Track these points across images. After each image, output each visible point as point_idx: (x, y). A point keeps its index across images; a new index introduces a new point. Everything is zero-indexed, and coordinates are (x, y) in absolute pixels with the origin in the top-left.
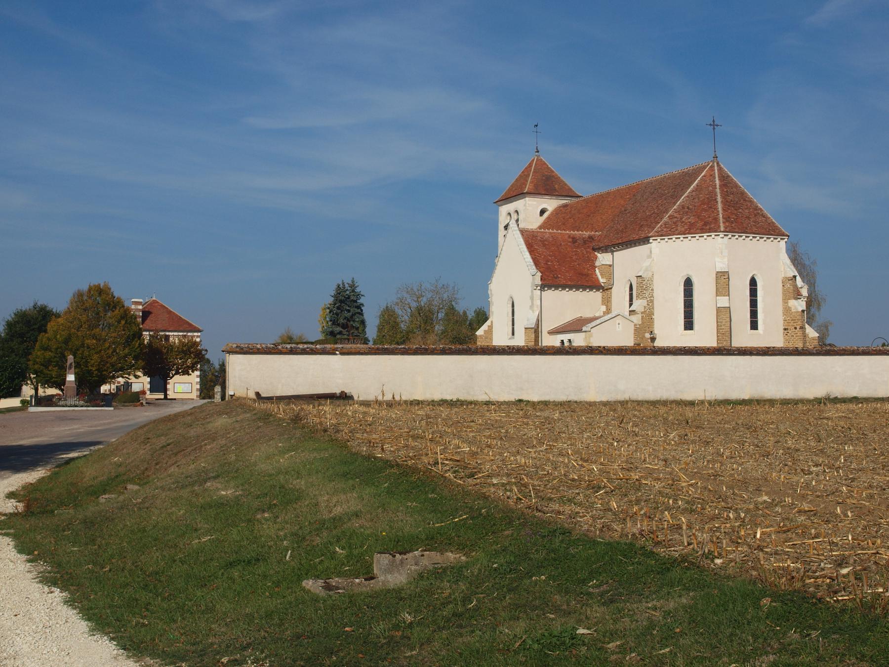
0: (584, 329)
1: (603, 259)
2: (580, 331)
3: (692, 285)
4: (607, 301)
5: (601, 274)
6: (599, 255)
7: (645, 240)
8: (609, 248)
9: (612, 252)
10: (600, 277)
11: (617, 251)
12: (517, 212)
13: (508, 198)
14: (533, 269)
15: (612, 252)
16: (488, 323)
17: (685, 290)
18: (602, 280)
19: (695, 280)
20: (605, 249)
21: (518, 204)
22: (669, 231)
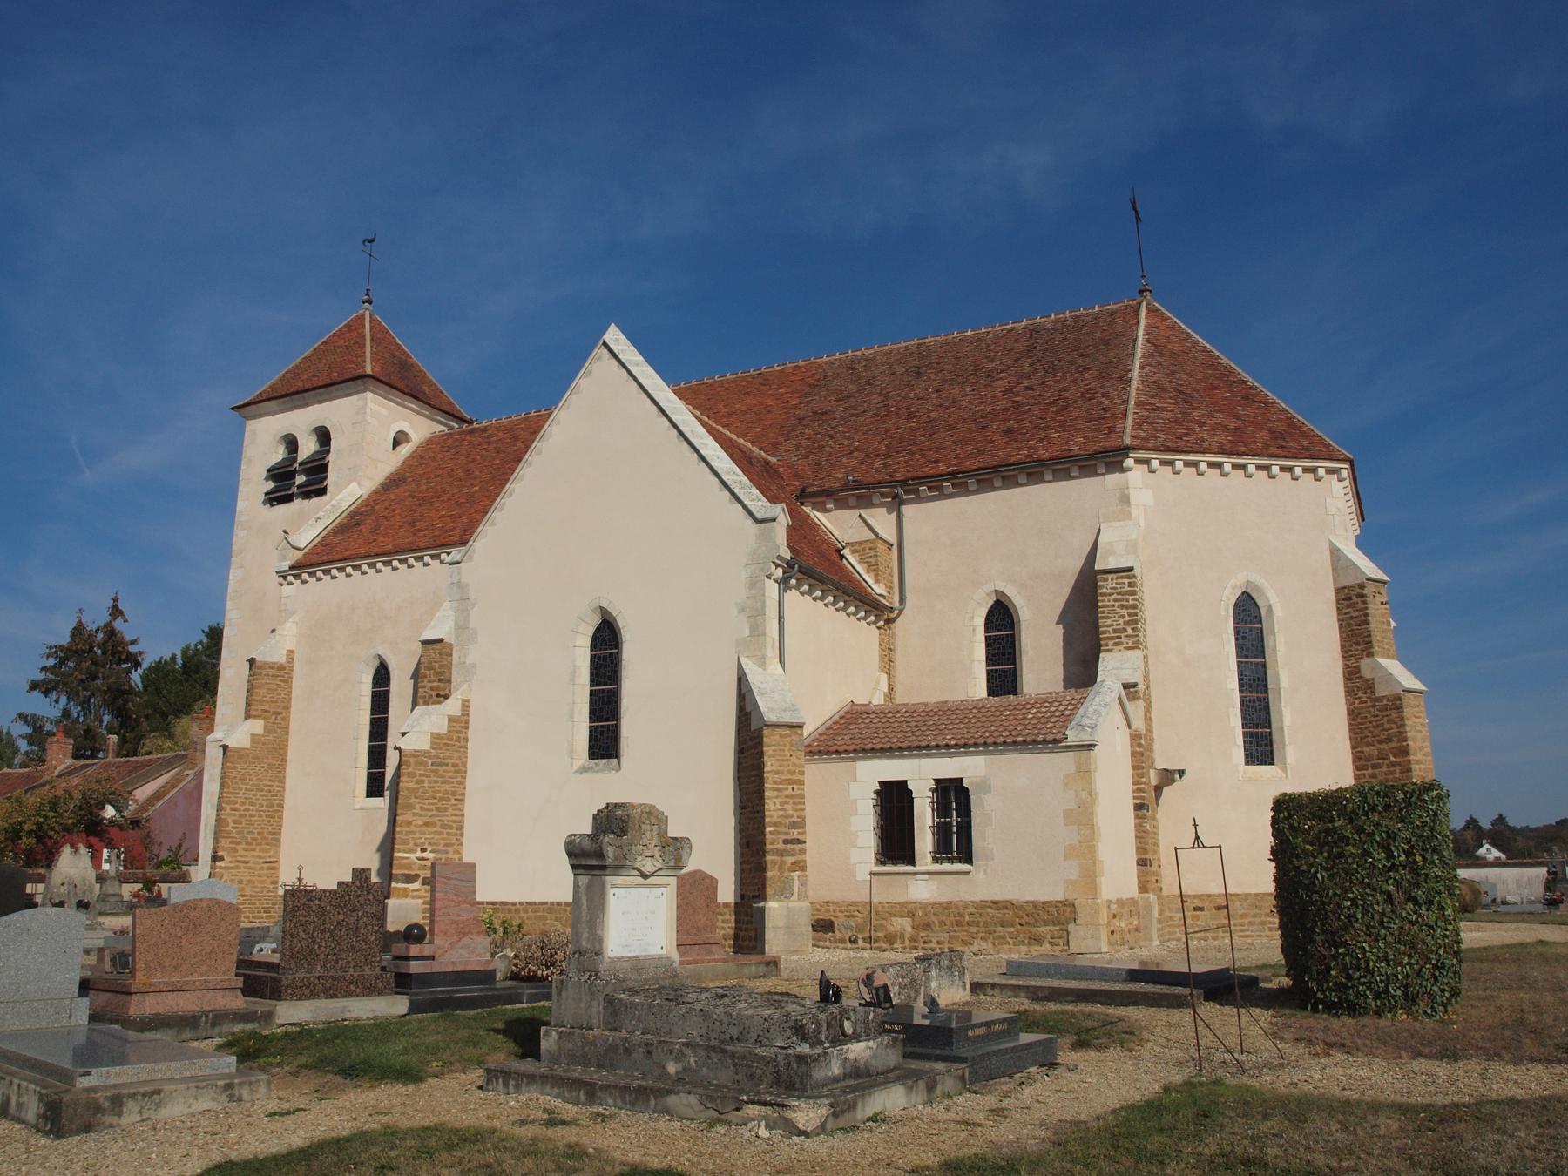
0: (1073, 737)
1: (882, 520)
2: (1055, 743)
3: (1258, 619)
4: (888, 662)
5: (873, 568)
6: (819, 517)
7: (1111, 459)
8: (900, 489)
9: (896, 504)
10: (869, 579)
11: (919, 500)
12: (324, 436)
13: (291, 393)
14: (757, 501)
15: (896, 504)
16: (452, 706)
17: (1237, 632)
18: (879, 589)
19: (1274, 601)
20: (856, 494)
21: (335, 412)
22: (1177, 437)
